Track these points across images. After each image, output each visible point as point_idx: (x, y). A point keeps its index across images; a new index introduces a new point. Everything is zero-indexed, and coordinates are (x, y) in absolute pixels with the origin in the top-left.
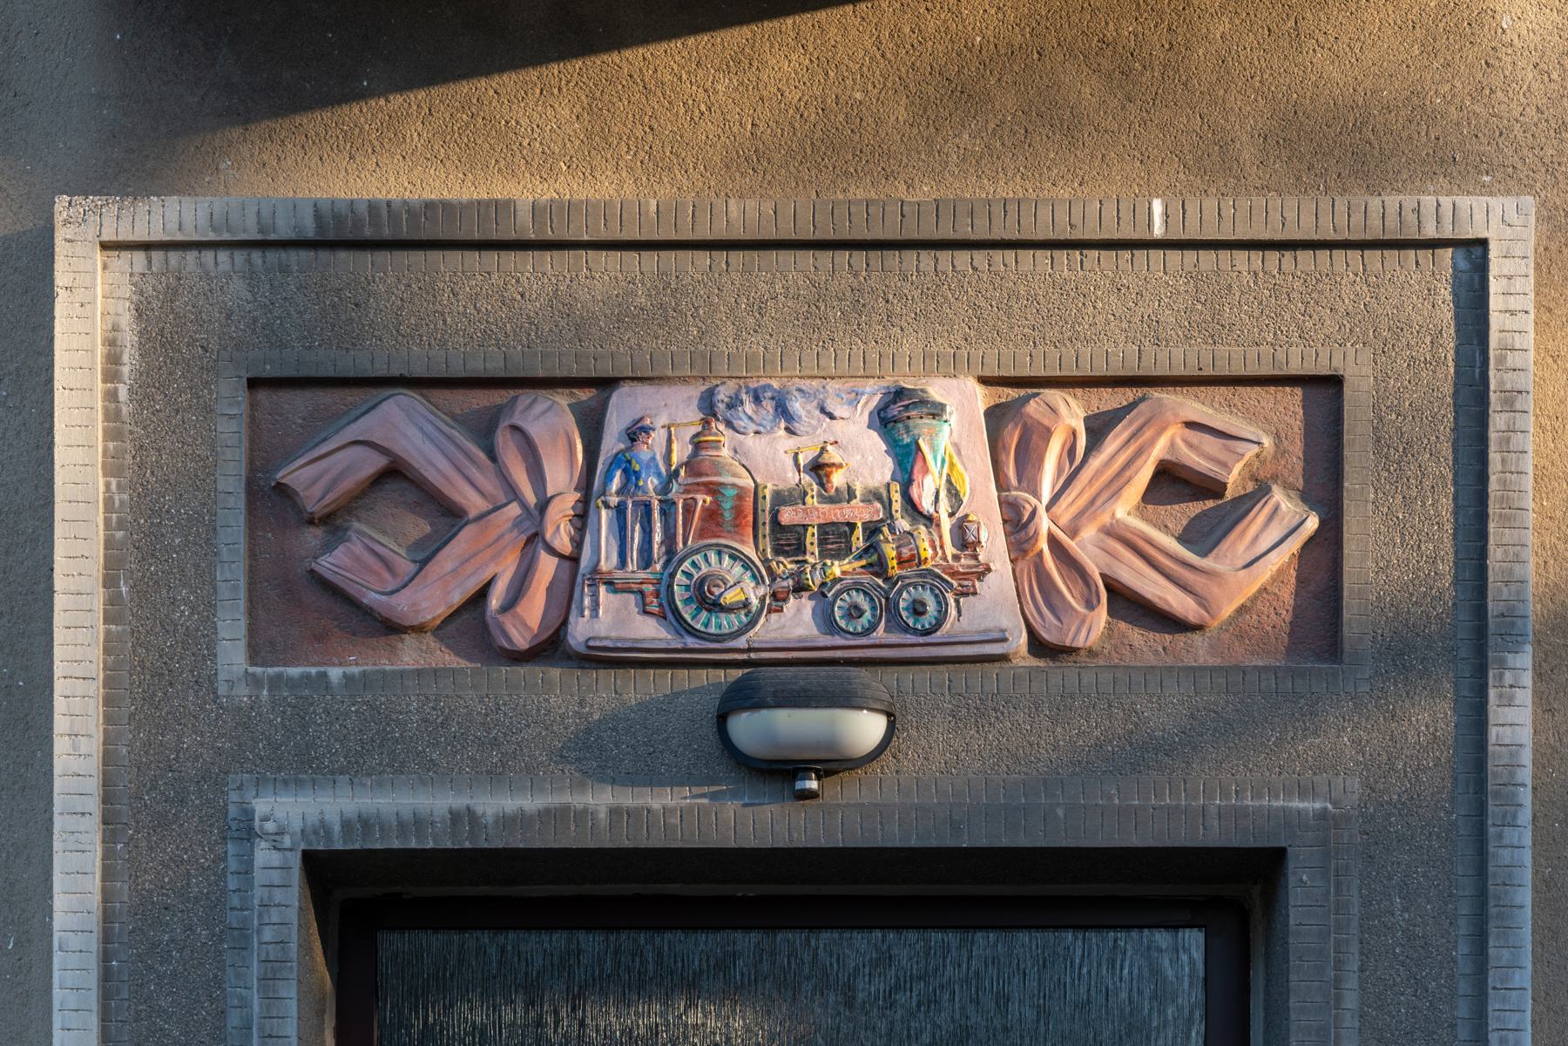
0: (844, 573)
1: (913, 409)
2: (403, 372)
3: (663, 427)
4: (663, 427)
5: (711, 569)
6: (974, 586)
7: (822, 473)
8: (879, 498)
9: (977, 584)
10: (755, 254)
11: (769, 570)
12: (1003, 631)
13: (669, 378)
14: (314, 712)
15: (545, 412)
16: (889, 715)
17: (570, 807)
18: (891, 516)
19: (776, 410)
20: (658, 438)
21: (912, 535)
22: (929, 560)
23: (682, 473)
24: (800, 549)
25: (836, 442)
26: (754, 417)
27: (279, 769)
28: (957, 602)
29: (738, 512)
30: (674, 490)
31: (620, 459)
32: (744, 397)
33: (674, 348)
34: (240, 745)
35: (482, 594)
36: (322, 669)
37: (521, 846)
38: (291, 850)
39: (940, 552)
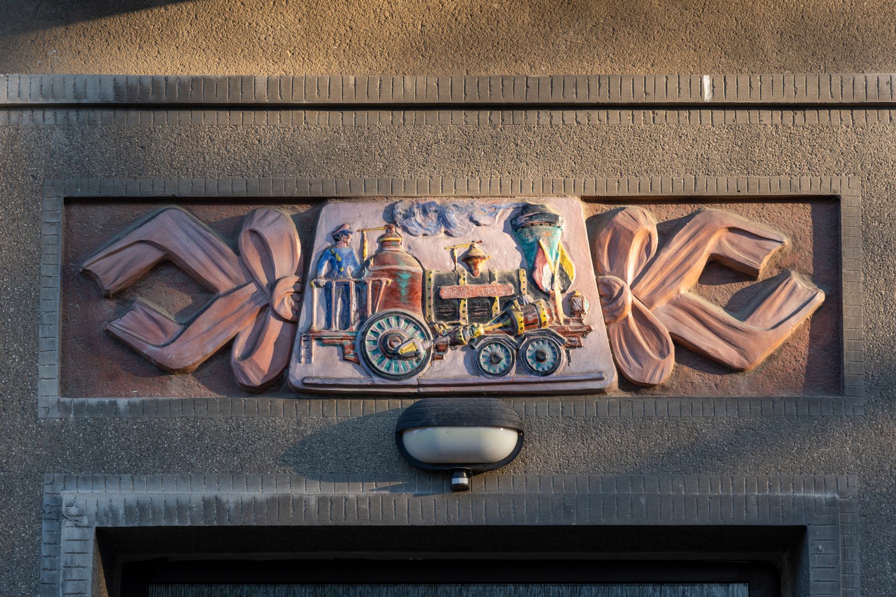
0: (486, 332)
1: (536, 219)
2: (174, 193)
3: (358, 231)
4: (358, 231)
5: (392, 329)
6: (579, 341)
7: (471, 262)
8: (512, 281)
9: (582, 340)
10: (423, 113)
11: (433, 330)
12: (600, 372)
13: (362, 198)
14: (107, 429)
15: (275, 221)
16: (519, 431)
17: (290, 496)
18: (520, 293)
19: (438, 220)
20: (354, 239)
21: (535, 306)
22: (548, 323)
23: (372, 262)
24: (456, 315)
25: (481, 242)
26: (423, 224)
27: (81, 470)
28: (567, 352)
29: (411, 290)
30: (365, 275)
31: (327, 253)
32: (416, 210)
33: (366, 177)
34: (53, 453)
35: (228, 347)
36: (113, 399)
37: (254, 524)
38: (88, 527)
39: (555, 318)
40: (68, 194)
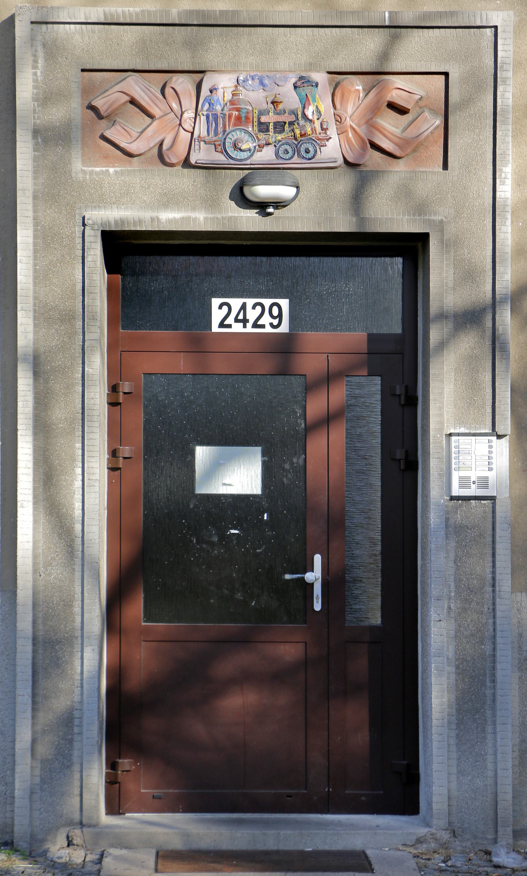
0: (282, 139)
3: (222, 88)
4: (222, 88)
6: (325, 143)
7: (275, 104)
8: (294, 114)
9: (327, 143)
12: (335, 159)
13: (223, 71)
14: (105, 183)
15: (182, 83)
16: (297, 187)
20: (220, 92)
23: (228, 104)
24: (268, 130)
27: (93, 202)
28: (320, 149)
32: (249, 78)
33: (225, 61)
34: (79, 194)
36: (107, 168)
38: (97, 230)
40: (82, 68)
